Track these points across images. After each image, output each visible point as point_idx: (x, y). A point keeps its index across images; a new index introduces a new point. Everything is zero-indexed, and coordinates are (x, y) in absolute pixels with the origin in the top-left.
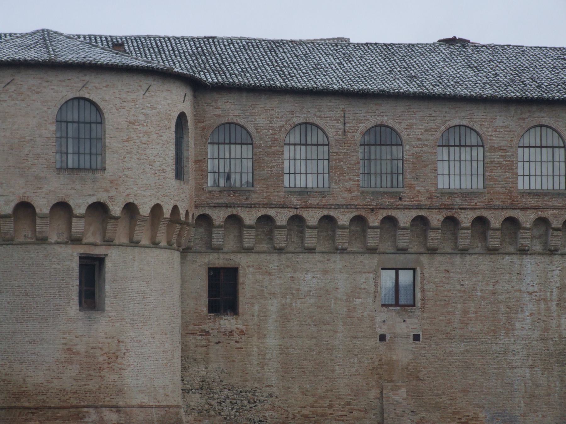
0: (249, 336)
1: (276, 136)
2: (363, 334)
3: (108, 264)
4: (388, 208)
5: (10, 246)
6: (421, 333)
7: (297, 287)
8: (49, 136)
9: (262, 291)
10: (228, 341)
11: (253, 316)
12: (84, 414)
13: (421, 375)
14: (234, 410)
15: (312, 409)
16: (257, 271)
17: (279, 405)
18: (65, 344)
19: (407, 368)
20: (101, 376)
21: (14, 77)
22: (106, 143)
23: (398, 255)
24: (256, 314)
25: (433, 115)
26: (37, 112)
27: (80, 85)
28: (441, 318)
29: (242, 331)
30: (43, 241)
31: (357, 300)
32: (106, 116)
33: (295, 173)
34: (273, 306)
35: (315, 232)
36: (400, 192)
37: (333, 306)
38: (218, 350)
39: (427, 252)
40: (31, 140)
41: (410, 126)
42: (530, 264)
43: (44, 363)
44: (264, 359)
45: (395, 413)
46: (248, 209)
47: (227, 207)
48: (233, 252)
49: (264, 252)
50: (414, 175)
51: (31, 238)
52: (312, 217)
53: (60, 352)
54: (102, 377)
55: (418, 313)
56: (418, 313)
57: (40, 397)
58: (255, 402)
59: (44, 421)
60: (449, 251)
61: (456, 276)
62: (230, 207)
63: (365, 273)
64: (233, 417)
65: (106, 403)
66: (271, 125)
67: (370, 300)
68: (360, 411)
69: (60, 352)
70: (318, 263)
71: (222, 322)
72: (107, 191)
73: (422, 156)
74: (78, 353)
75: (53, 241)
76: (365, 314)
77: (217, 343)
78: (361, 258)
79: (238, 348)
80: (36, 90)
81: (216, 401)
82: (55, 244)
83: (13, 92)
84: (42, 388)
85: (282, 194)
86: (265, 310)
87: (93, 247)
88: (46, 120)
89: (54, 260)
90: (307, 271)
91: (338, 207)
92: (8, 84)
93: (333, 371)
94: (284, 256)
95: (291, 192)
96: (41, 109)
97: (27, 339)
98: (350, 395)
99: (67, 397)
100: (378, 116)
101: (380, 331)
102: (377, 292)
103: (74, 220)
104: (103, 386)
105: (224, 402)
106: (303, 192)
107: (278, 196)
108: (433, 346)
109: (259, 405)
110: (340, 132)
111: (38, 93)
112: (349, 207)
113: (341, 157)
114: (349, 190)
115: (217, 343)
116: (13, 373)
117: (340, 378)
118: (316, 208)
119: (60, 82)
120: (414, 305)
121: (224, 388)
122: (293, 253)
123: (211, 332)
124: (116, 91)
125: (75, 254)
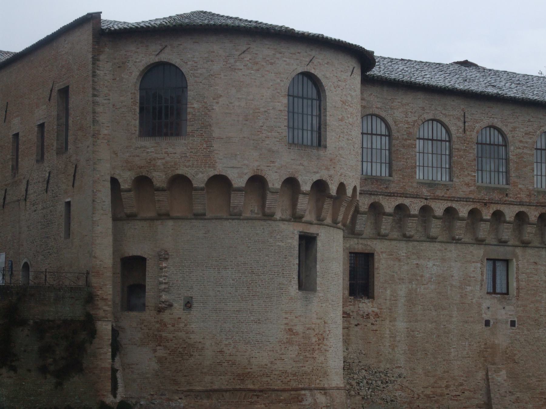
0: (383, 319)
1: (411, 130)
2: (472, 319)
3: (319, 244)
4: (498, 203)
5: (236, 221)
6: (516, 320)
7: (421, 274)
8: (282, 109)
9: (393, 275)
10: (365, 324)
11: (386, 300)
12: (303, 397)
13: (516, 357)
14: (370, 390)
15: (433, 390)
16: (388, 257)
17: (407, 385)
18: (286, 324)
19: (506, 351)
20: (313, 358)
21: (249, 46)
22: (328, 121)
23: (499, 247)
24: (388, 298)
25: (531, 120)
26: (271, 84)
27: (308, 60)
28: (532, 306)
29: (377, 314)
30: (268, 217)
31: (468, 287)
33: (423, 166)
34: (402, 291)
35: (439, 223)
36: (507, 189)
37: (449, 292)
38: (357, 331)
39: (521, 245)
40: (265, 111)
41: (514, 129)
43: (268, 343)
44: (395, 341)
45: (500, 394)
46: (387, 197)
47: (371, 194)
48: (370, 238)
49: (395, 240)
50: (517, 174)
51: (257, 214)
52: (439, 208)
53: (283, 332)
54: (314, 358)
55: (514, 301)
56: (514, 301)
57: (265, 379)
58: (387, 382)
59: (269, 404)
60: (537, 244)
61: (542, 268)
62: (374, 194)
63: (474, 262)
64: (369, 397)
65: (317, 386)
66: (406, 119)
67: (478, 287)
68: (471, 391)
69: (283, 332)
70: (438, 252)
71: (361, 305)
72: (328, 169)
73: (523, 157)
74: (297, 334)
75: (278, 218)
76: (474, 301)
77: (356, 325)
79: (373, 330)
80: (270, 61)
81: (355, 381)
82: (279, 220)
83: (248, 61)
84: (267, 371)
85: (415, 185)
86: (395, 294)
87: (309, 226)
88: (279, 93)
89: (278, 237)
90: (429, 259)
91: (459, 200)
92: (244, 52)
93: (449, 354)
94: (411, 244)
95: (422, 183)
96: (274, 80)
97: (252, 319)
98: (462, 376)
99: (288, 379)
100: (490, 118)
101: (486, 317)
102: (483, 280)
103: (301, 197)
104: (314, 368)
105: (361, 382)
106: (432, 185)
107: (412, 186)
108: (526, 332)
109: (390, 386)
110: (461, 130)
111: (272, 64)
112: (468, 200)
113: (462, 153)
114: (468, 185)
115: (356, 325)
116: (238, 353)
117: (455, 360)
118: (441, 200)
119: (291, 55)
120: (507, 293)
121: (362, 369)
122: (418, 241)
123: (351, 314)
124: (334, 69)
125: (296, 232)
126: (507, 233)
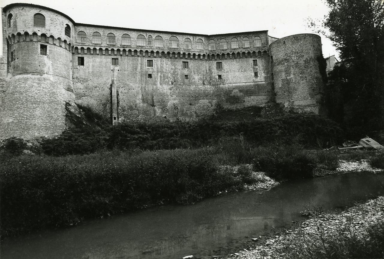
32: (46, 18)
34: (91, 64)
42: (139, 58)
52: (98, 48)
78: (108, 56)
101: (112, 69)
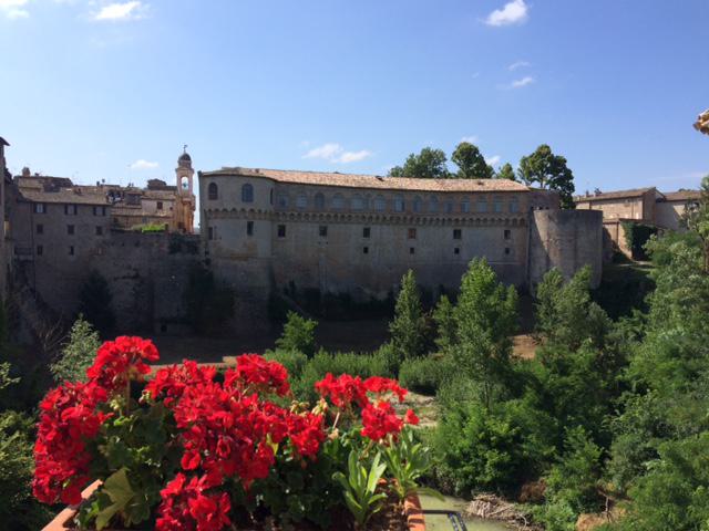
30: (238, 218)
42: (354, 227)
106: (301, 208)
126: (325, 219)
